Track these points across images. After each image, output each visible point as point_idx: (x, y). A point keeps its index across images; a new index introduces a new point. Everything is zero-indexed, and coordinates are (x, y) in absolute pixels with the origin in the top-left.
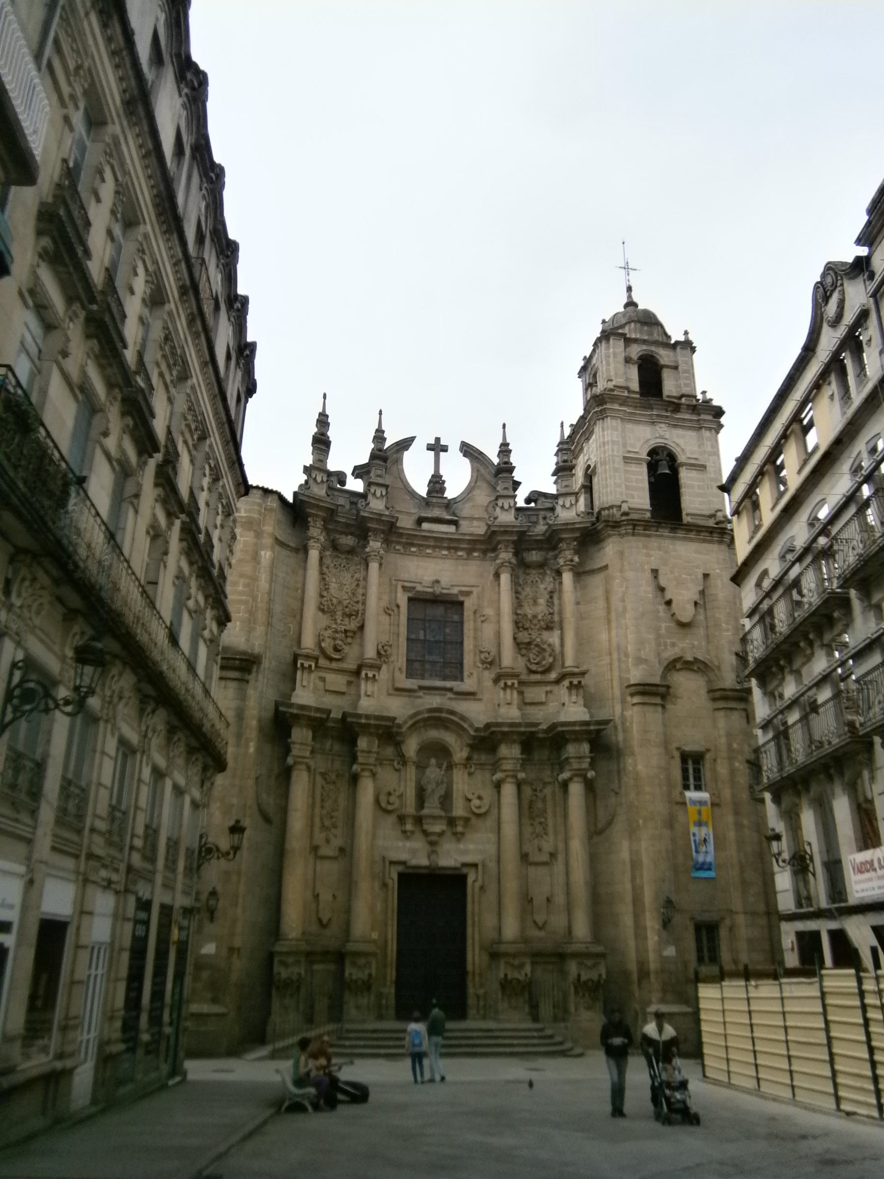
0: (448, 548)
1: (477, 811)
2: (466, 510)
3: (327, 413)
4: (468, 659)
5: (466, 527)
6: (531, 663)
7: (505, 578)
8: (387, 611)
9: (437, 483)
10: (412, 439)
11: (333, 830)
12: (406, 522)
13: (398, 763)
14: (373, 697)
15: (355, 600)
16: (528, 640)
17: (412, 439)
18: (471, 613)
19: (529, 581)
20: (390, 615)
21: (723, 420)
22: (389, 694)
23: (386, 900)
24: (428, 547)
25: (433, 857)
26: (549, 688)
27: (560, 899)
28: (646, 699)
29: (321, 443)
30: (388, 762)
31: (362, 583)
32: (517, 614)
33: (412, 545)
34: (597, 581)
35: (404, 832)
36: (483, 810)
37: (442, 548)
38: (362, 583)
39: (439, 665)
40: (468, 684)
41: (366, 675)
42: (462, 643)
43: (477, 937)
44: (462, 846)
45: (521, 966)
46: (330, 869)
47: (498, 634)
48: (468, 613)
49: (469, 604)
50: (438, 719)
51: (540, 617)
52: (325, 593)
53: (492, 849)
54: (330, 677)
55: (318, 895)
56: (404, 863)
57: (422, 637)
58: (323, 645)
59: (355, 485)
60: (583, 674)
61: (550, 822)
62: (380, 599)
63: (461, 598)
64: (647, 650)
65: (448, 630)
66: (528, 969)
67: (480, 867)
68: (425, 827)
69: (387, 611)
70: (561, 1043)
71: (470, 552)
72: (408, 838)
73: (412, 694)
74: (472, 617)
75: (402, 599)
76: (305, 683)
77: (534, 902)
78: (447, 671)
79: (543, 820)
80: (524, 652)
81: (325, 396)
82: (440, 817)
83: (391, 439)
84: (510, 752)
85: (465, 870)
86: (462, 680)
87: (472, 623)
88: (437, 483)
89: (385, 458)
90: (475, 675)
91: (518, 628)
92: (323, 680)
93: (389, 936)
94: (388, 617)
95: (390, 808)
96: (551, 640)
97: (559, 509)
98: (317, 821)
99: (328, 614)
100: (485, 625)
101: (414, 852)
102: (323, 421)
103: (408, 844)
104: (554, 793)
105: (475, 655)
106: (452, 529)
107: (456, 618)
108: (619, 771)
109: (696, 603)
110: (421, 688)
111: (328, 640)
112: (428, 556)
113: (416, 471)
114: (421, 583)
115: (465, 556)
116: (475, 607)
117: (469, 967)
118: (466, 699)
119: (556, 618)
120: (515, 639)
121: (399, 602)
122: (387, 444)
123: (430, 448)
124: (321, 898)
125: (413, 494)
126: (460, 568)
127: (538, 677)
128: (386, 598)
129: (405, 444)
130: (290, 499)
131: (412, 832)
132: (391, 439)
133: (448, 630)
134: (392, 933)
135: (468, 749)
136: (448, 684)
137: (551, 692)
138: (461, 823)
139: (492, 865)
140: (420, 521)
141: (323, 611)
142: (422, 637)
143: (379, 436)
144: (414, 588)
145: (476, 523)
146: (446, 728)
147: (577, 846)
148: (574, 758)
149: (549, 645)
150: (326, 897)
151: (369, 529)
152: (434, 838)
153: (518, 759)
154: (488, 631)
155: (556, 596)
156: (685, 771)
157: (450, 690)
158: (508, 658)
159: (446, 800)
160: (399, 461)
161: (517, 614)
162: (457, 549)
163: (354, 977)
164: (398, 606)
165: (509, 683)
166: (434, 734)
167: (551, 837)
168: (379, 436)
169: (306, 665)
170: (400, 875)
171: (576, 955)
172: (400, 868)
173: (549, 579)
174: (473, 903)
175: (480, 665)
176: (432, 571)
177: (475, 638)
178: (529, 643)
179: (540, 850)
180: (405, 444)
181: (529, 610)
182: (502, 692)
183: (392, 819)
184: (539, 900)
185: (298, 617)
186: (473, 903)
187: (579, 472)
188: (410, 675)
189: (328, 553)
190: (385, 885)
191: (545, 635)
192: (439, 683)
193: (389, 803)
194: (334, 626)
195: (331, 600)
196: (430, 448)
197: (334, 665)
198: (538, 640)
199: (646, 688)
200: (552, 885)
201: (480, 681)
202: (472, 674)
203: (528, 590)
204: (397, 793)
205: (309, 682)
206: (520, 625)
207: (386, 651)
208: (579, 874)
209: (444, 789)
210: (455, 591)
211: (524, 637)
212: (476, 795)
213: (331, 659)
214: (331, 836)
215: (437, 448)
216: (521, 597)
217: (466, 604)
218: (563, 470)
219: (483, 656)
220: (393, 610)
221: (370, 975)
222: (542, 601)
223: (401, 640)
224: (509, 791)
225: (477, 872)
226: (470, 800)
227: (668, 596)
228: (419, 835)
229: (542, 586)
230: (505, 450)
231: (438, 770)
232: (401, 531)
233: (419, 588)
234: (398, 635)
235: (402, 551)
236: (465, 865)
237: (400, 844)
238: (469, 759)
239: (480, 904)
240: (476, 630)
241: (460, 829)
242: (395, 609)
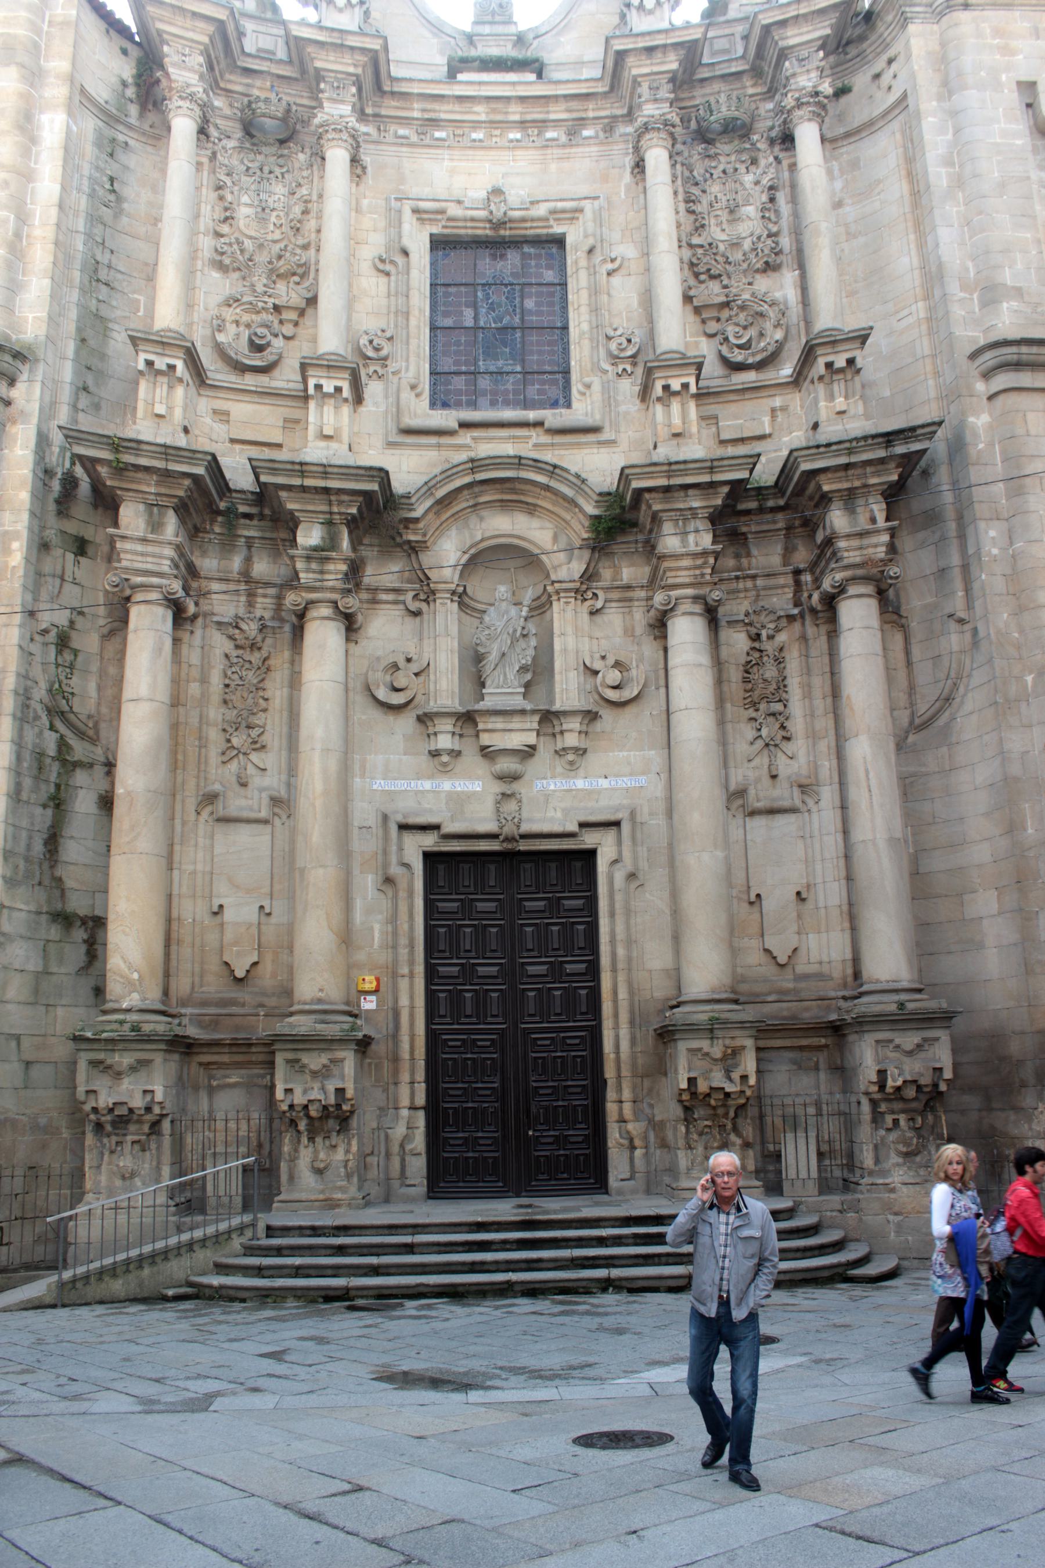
0: (523, 124)
1: (612, 695)
4: (581, 353)
6: (732, 347)
7: (657, 157)
8: (382, 267)
11: (254, 757)
13: (415, 596)
14: (341, 442)
15: (300, 241)
16: (723, 299)
18: (582, 254)
19: (717, 173)
20: (388, 274)
22: (391, 445)
23: (393, 919)
24: (476, 125)
25: (511, 806)
26: (777, 402)
27: (831, 894)
28: (1026, 379)
30: (390, 597)
31: (314, 207)
32: (691, 246)
33: (434, 123)
34: (883, 150)
35: (435, 754)
36: (627, 694)
37: (505, 125)
39: (511, 378)
40: (583, 409)
41: (318, 387)
42: (565, 328)
43: (623, 994)
44: (580, 784)
45: (732, 1055)
47: (648, 300)
48: (575, 256)
49: (574, 236)
50: (505, 486)
51: (747, 245)
53: (652, 786)
54: (241, 410)
55: (221, 906)
56: (436, 827)
57: (469, 322)
58: (221, 338)
60: (862, 338)
61: (797, 707)
63: (557, 229)
64: (1019, 266)
65: (530, 304)
66: (749, 1064)
67: (626, 827)
68: (485, 739)
69: (382, 267)
70: (838, 1246)
71: (574, 128)
72: (445, 770)
73: (445, 440)
74: (583, 263)
75: (418, 241)
77: (767, 904)
78: (532, 391)
79: (779, 707)
80: (713, 327)
82: (523, 712)
84: (684, 540)
85: (589, 840)
86: (569, 406)
87: (583, 275)
90: (597, 387)
91: (697, 275)
92: (222, 416)
93: (404, 1001)
94: (383, 280)
95: (397, 699)
96: (778, 295)
98: (214, 735)
99: (236, 275)
100: (616, 280)
101: (459, 800)
103: (447, 785)
105: (595, 348)
107: (549, 276)
108: (965, 568)
110: (464, 425)
111: (232, 329)
112: (477, 145)
114: (459, 202)
115: (564, 139)
116: (591, 241)
118: (579, 445)
119: (786, 242)
120: (687, 299)
121: (406, 242)
124: (228, 915)
126: (553, 167)
127: (750, 377)
131: (456, 754)
133: (530, 304)
135: (586, 554)
136: (532, 415)
137: (784, 409)
138: (574, 724)
139: (657, 823)
142: (469, 322)
144: (442, 212)
146: (531, 509)
147: (868, 754)
148: (848, 536)
149: (773, 304)
152: (506, 765)
153: (705, 553)
154: (624, 294)
155: (781, 197)
157: (539, 424)
158: (675, 331)
159: (538, 672)
161: (691, 246)
162: (542, 124)
163: (299, 1099)
164: (406, 253)
165: (676, 385)
166: (501, 525)
167: (799, 746)
170: (430, 858)
171: (879, 1021)
172: (429, 841)
173: (766, 160)
174: (612, 914)
175: (606, 366)
177: (595, 310)
178: (726, 305)
179: (774, 777)
181: (717, 233)
182: (659, 408)
183: (406, 723)
184: (778, 901)
186: (612, 914)
188: (438, 401)
190: (389, 880)
191: (763, 284)
192: (509, 414)
194: (245, 299)
195: (239, 242)
197: (250, 381)
198: (746, 296)
199: (1024, 349)
200: (807, 862)
201: (609, 400)
202: (588, 386)
203: (715, 189)
204: (415, 667)
206: (702, 268)
207: (377, 350)
208: (877, 817)
209: (531, 652)
210: (541, 210)
211: (713, 293)
212: (611, 661)
213: (242, 369)
214: (251, 770)
216: (698, 208)
217: (569, 240)
219: (613, 346)
220: (392, 262)
221: (340, 1092)
222: (750, 210)
223: (413, 322)
224: (687, 631)
225: (619, 842)
226: (596, 673)
228: (471, 759)
229: (748, 179)
231: (513, 611)
232: (404, 88)
233: (454, 210)
234: (407, 315)
235: (414, 138)
236: (582, 825)
237: (427, 785)
238: (589, 576)
239: (628, 912)
240: (595, 291)
241: (571, 740)
242: (400, 260)
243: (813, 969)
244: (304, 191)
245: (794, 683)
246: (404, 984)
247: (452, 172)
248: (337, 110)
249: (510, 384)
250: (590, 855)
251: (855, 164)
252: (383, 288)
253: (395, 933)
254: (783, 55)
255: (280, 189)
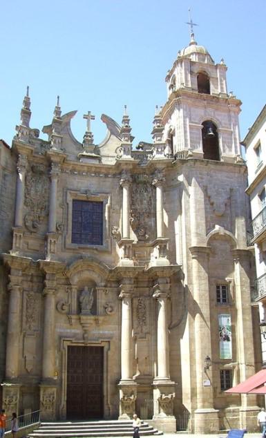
2: (104, 152)
3: (29, 97)
5: (105, 161)
9: (88, 135)
10: (76, 112)
12: (71, 158)
17: (76, 112)
19: (139, 192)
21: (241, 107)
23: (61, 360)
29: (26, 114)
31: (47, 191)
38: (49, 191)
43: (109, 378)
46: (31, 342)
52: (27, 196)
54: (31, 242)
58: (27, 224)
59: (44, 137)
62: (58, 200)
70: (152, 429)
76: (17, 245)
81: (28, 87)
83: (64, 112)
85: (102, 345)
88: (88, 135)
89: (61, 123)
97: (155, 153)
98: (24, 318)
100: (114, 214)
102: (27, 102)
104: (150, 304)
106: (96, 162)
109: (226, 205)
113: (78, 130)
117: (105, 394)
121: (68, 202)
122: (62, 115)
123: (85, 117)
124: (27, 358)
125: (76, 142)
128: (61, 199)
129: (72, 114)
130: (10, 145)
132: (64, 112)
133: (94, 217)
134: (65, 376)
140: (79, 159)
141: (27, 206)
143: (58, 111)
145: (110, 159)
150: (29, 357)
151: (52, 162)
156: (218, 292)
160: (68, 124)
164: (68, 204)
168: (58, 111)
169: (18, 234)
176: (84, 184)
180: (72, 114)
185: (13, 209)
187: (165, 132)
189: (29, 174)
193: (62, 309)
196: (85, 117)
197: (33, 235)
205: (19, 244)
215: (89, 117)
218: (157, 132)
227: (212, 201)
229: (145, 194)
230: (126, 120)
237: (69, 331)
243: (148, 373)
244: (45, 187)
245: (148, 313)
246: (63, 374)
247: (78, 182)
248: (55, 170)
249: (89, 237)
250: (102, 348)
251: (168, 195)
252: (62, 212)
253: (62, 363)
254: (156, 169)
255: (40, 186)
